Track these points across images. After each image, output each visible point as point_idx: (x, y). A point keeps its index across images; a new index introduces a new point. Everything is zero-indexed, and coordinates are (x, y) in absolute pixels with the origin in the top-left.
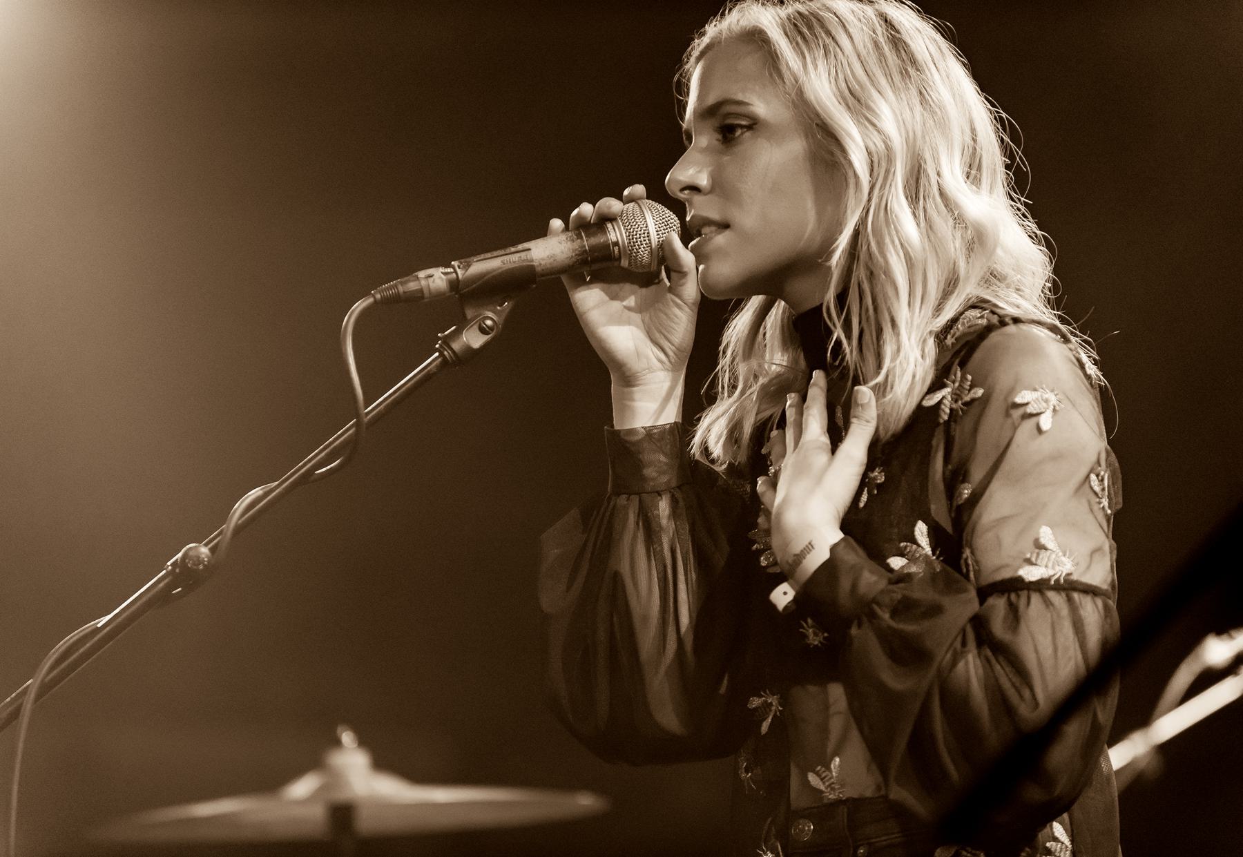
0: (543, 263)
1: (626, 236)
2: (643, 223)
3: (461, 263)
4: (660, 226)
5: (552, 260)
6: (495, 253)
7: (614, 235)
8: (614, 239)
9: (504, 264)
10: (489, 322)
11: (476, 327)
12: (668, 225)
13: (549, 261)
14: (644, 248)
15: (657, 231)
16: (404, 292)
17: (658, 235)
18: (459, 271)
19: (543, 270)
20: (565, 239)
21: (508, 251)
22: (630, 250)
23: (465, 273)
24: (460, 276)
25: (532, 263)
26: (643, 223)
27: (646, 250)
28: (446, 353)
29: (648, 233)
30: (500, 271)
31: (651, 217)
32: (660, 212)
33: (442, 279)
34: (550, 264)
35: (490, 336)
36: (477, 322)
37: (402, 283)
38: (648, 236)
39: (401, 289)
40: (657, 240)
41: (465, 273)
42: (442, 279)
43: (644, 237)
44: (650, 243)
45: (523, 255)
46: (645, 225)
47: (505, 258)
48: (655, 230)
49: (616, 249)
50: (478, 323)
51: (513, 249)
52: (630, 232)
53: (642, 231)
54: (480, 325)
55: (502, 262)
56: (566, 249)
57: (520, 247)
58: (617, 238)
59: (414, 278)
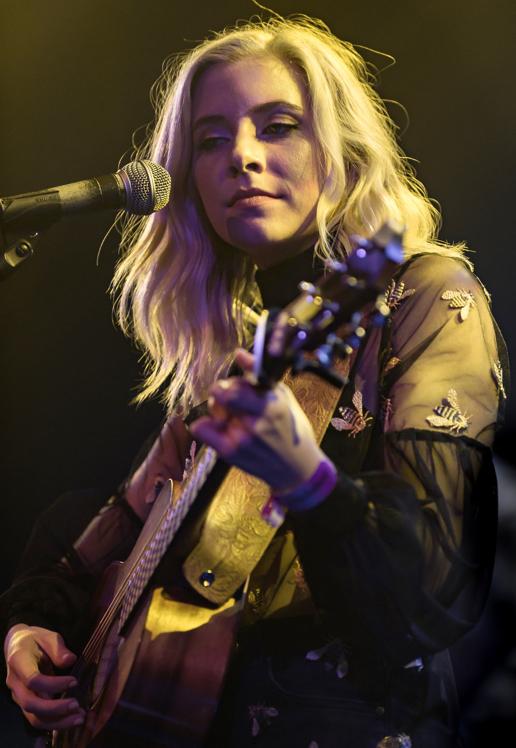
0: (67, 202)
2: (145, 176)
3: (4, 200)
5: (74, 201)
6: (30, 194)
7: (122, 184)
9: (38, 201)
12: (164, 179)
14: (145, 195)
15: (156, 183)
17: (156, 186)
20: (84, 185)
21: (40, 192)
22: (134, 197)
23: (7, 208)
24: (4, 209)
25: (60, 203)
26: (145, 176)
27: (146, 197)
29: (149, 184)
30: (35, 207)
31: (151, 170)
36: (16, 245)
38: (148, 187)
40: (155, 189)
41: (7, 208)
43: (146, 187)
45: (53, 195)
46: (146, 178)
48: (154, 182)
51: (44, 191)
52: (134, 183)
55: (36, 200)
56: (85, 194)
57: (50, 190)
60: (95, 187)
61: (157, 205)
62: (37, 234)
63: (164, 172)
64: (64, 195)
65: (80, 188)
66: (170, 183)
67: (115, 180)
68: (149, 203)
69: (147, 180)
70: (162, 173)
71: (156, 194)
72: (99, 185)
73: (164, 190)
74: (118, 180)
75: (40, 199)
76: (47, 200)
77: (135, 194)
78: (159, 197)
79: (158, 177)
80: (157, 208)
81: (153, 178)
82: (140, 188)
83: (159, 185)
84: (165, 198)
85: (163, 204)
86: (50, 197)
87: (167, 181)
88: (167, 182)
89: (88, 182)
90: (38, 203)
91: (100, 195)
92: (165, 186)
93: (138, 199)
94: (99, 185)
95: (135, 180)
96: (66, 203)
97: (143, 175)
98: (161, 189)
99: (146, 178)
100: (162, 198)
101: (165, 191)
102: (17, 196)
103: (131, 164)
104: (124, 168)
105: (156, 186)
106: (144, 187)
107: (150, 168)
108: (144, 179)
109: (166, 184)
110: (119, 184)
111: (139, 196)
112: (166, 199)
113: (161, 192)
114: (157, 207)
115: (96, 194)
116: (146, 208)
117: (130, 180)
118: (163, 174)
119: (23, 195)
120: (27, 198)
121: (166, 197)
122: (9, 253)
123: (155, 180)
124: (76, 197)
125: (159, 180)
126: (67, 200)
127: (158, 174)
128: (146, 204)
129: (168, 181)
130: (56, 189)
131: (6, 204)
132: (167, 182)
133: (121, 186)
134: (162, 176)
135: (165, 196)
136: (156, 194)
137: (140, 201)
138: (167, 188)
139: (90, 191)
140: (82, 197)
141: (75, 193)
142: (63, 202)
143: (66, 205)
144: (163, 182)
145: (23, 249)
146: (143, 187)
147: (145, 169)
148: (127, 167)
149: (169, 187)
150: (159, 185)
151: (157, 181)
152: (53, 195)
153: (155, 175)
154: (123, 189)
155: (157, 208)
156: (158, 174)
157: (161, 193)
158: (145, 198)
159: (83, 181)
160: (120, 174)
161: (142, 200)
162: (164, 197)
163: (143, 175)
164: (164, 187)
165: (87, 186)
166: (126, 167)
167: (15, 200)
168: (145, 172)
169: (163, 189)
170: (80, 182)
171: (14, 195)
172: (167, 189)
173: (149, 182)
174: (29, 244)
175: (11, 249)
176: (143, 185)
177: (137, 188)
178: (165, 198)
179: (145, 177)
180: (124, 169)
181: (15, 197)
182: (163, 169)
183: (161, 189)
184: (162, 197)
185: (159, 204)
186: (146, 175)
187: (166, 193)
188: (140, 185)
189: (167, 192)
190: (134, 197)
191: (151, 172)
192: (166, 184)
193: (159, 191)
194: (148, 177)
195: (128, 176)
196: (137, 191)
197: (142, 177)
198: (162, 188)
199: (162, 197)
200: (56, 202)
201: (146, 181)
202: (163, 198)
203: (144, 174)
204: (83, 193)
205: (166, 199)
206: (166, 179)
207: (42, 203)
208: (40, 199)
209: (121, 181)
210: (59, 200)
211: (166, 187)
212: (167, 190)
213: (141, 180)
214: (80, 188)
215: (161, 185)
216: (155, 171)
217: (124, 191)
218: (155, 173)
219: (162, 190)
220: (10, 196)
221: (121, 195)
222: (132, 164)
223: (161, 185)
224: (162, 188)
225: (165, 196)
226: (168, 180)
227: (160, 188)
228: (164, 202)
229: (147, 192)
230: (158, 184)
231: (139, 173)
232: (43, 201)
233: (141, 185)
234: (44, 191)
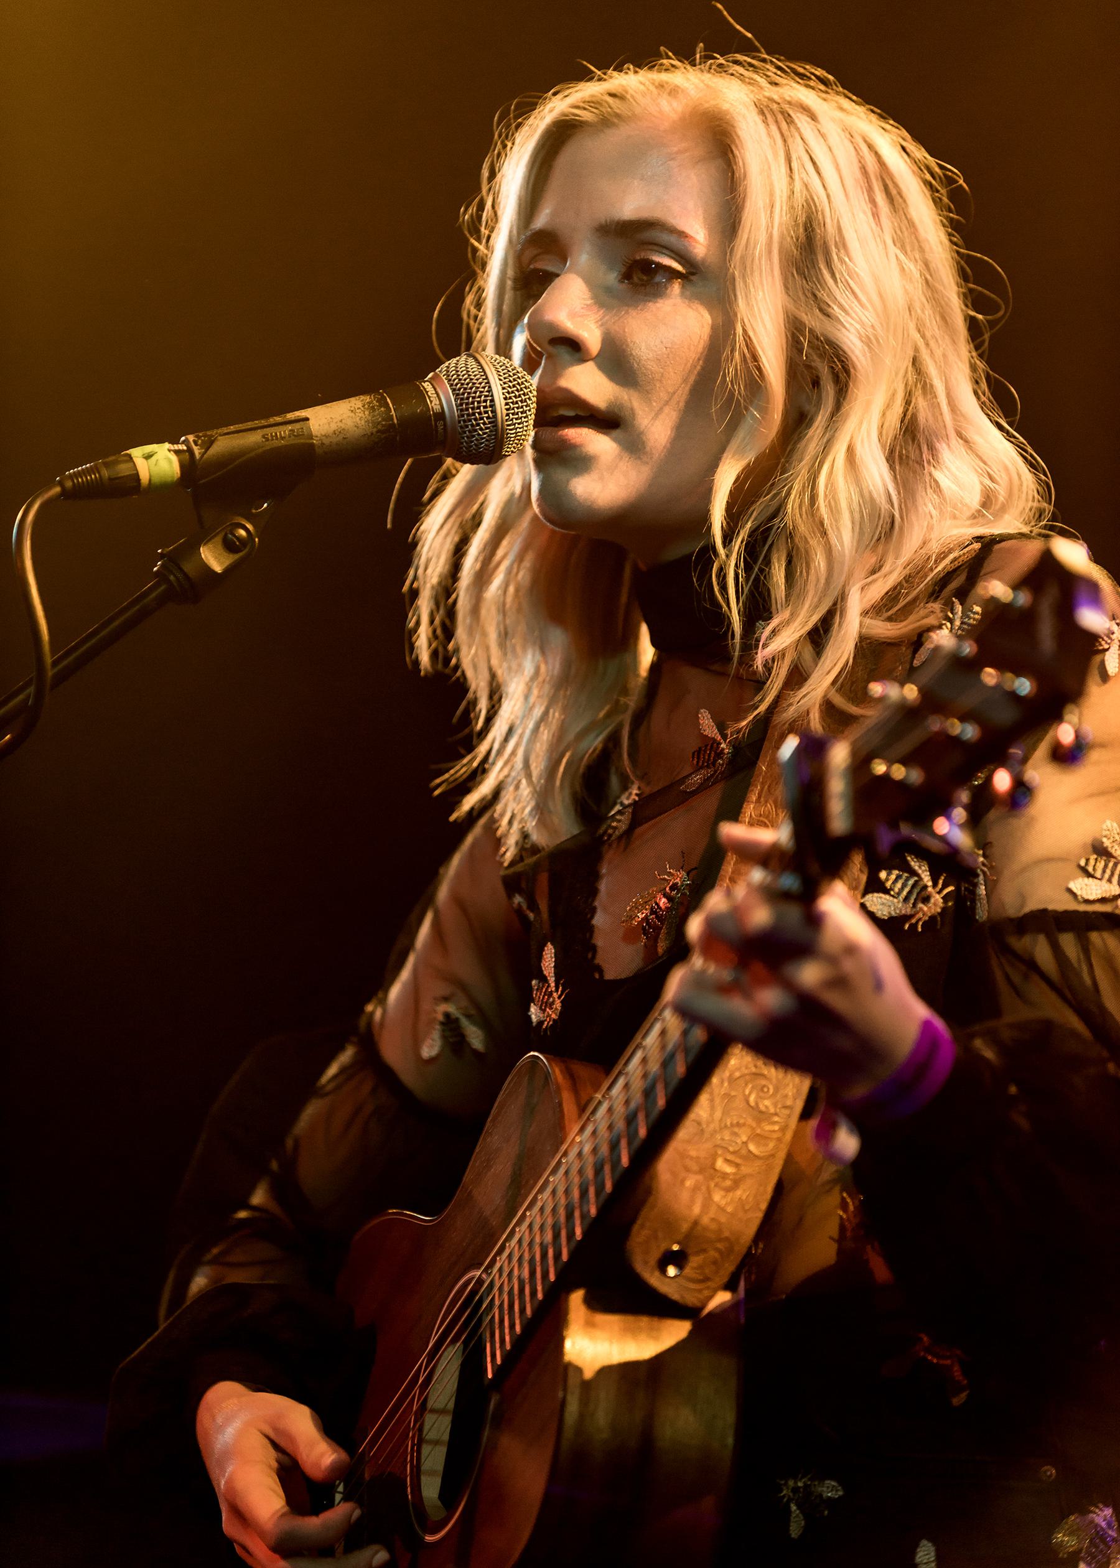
0: (326, 441)
1: (457, 406)
2: (483, 385)
3: (196, 436)
4: (510, 390)
6: (250, 425)
7: (438, 403)
8: (437, 408)
9: (267, 440)
10: (243, 533)
11: (219, 539)
13: (335, 440)
14: (484, 424)
15: (505, 399)
16: (110, 479)
18: (197, 451)
19: (326, 453)
20: (360, 406)
21: (272, 420)
22: (461, 427)
24: (197, 456)
25: (311, 441)
26: (483, 385)
27: (486, 428)
28: (172, 578)
29: (492, 401)
30: (261, 450)
31: (495, 373)
32: (510, 369)
33: (170, 461)
34: (337, 444)
35: (241, 554)
37: (106, 465)
38: (491, 406)
39: (105, 473)
40: (505, 412)
41: (205, 452)
42: (170, 461)
43: (485, 407)
44: (495, 416)
46: (486, 389)
47: (268, 431)
48: (502, 397)
49: (440, 424)
50: (223, 533)
51: (278, 419)
52: (462, 399)
53: (483, 398)
54: (226, 535)
55: (263, 437)
56: (363, 422)
57: (291, 416)
58: (441, 404)
59: (125, 458)
60: (382, 409)
61: (509, 444)
62: (265, 505)
63: (523, 378)
64: (320, 425)
65: (352, 411)
66: (534, 399)
67: (422, 395)
68: (493, 439)
69: (487, 394)
70: (519, 378)
71: (507, 420)
72: (391, 405)
73: (522, 413)
74: (429, 393)
75: (271, 434)
76: (284, 437)
77: (464, 421)
78: (513, 427)
79: (509, 387)
80: (508, 450)
81: (500, 388)
82: (473, 409)
83: (512, 403)
84: (525, 428)
85: (521, 441)
86: (290, 430)
87: (528, 394)
88: (527, 397)
89: (367, 398)
90: (267, 443)
91: (394, 424)
92: (525, 404)
93: (469, 431)
94: (391, 405)
95: (463, 394)
96: (324, 442)
97: (480, 383)
98: (516, 410)
99: (486, 389)
100: (518, 430)
101: (524, 415)
102: (225, 430)
103: (454, 360)
104: (440, 369)
105: (507, 404)
106: (482, 408)
107: (493, 369)
108: (481, 392)
109: (526, 401)
110: (431, 402)
111: (472, 425)
112: (526, 431)
113: (517, 416)
114: (508, 448)
115: (384, 423)
116: (485, 449)
117: (453, 395)
118: (520, 381)
119: (237, 426)
120: (244, 433)
121: (527, 426)
122: (210, 545)
123: (503, 394)
124: (343, 429)
125: (513, 392)
126: (325, 435)
127: (510, 381)
128: (487, 440)
129: (531, 395)
130: (302, 413)
131: (201, 446)
132: (527, 397)
133: (435, 407)
134: (518, 384)
135: (525, 424)
136: (507, 420)
137: (474, 436)
138: (528, 408)
139: (374, 416)
140: (356, 428)
141: (341, 421)
142: (317, 441)
143: (324, 446)
144: (520, 396)
145: (238, 538)
146: (479, 408)
147: (484, 371)
148: (448, 367)
149: (532, 406)
150: (512, 403)
151: (508, 396)
152: (297, 426)
153: (505, 383)
154: (439, 413)
155: (508, 450)
156: (510, 381)
157: (516, 419)
158: (483, 430)
159: (357, 398)
160: (433, 382)
161: (479, 434)
162: (523, 427)
163: (480, 383)
164: (522, 407)
165: (366, 406)
166: (444, 367)
167: (219, 438)
168: (484, 377)
169: (521, 410)
170: (352, 399)
171: (218, 428)
172: (529, 410)
173: (492, 396)
174: (250, 526)
175: (215, 536)
176: (479, 402)
177: (467, 409)
178: (525, 428)
179: (484, 388)
180: (440, 371)
181: (219, 431)
182: (519, 370)
183: (516, 410)
184: (520, 428)
185: (513, 441)
186: (486, 383)
187: (526, 420)
188: (473, 403)
189: (530, 417)
190: (461, 427)
191: (496, 376)
192: (526, 401)
193: (513, 414)
194: (490, 387)
195: (448, 386)
196: (468, 415)
197: (478, 388)
198: (518, 408)
199: (520, 428)
200: (302, 441)
201: (486, 396)
202: (521, 430)
203: (480, 380)
204: (359, 422)
205: (526, 431)
206: (526, 391)
207: (276, 443)
208: (271, 434)
209: (435, 395)
210: (311, 436)
211: (526, 406)
212: (528, 413)
213: (475, 392)
214: (352, 411)
215: (517, 403)
216: (504, 374)
217: (441, 415)
218: (505, 378)
219: (517, 414)
220: (212, 428)
221: (436, 424)
222: (458, 361)
223: (517, 403)
224: (518, 408)
225: (525, 424)
226: (530, 391)
227: (513, 409)
228: (523, 437)
229: (488, 418)
230: (511, 401)
231: (471, 379)
232: (277, 439)
233: (476, 403)
234: (278, 419)
